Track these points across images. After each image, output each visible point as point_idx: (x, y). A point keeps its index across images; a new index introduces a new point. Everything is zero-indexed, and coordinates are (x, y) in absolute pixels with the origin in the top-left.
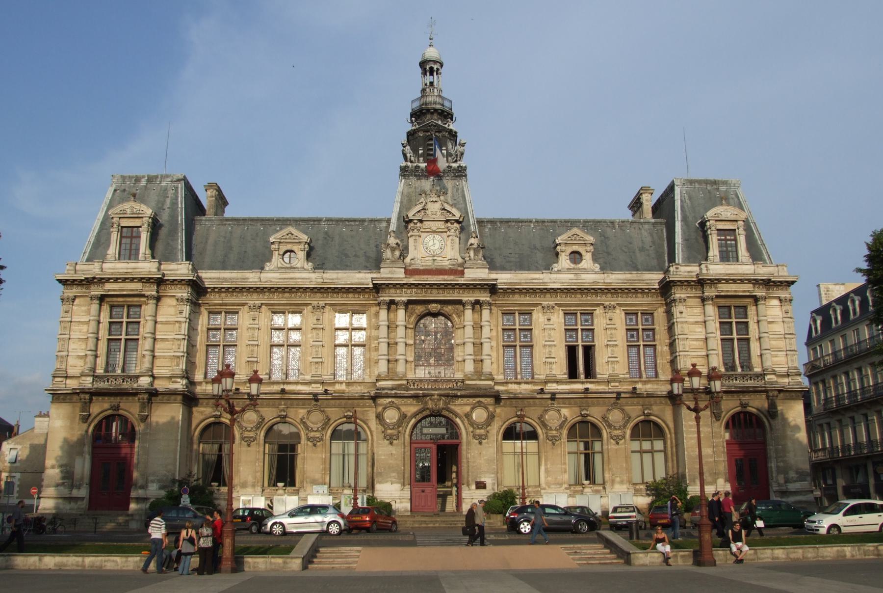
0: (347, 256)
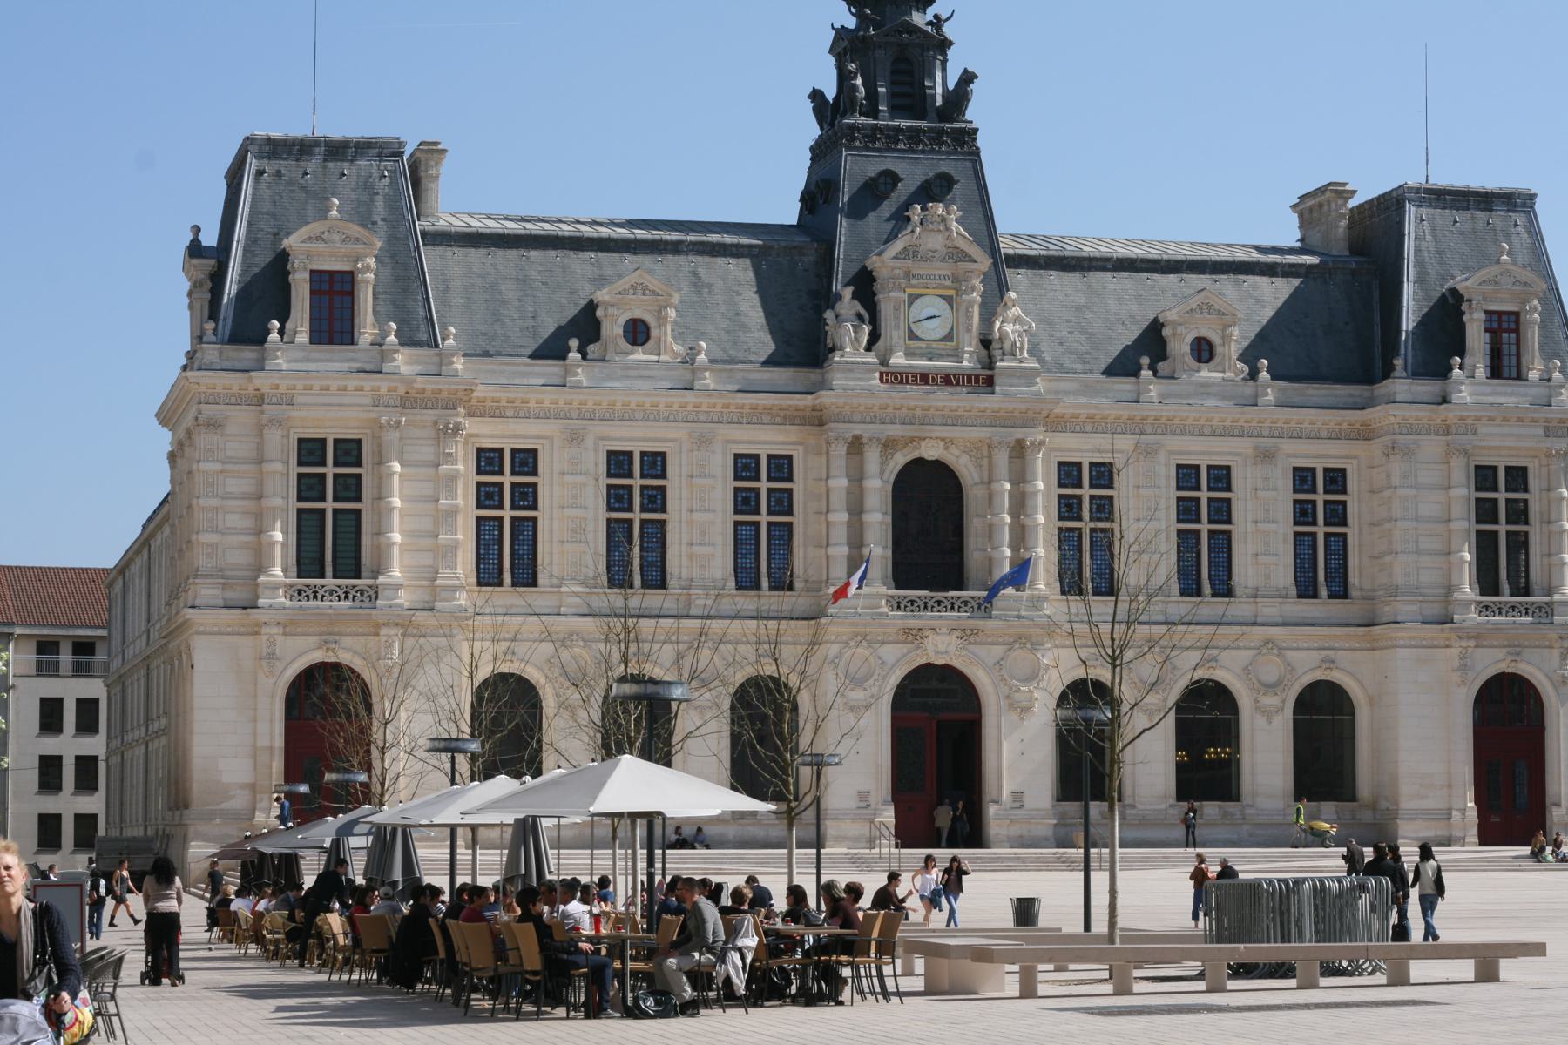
0: (744, 328)
